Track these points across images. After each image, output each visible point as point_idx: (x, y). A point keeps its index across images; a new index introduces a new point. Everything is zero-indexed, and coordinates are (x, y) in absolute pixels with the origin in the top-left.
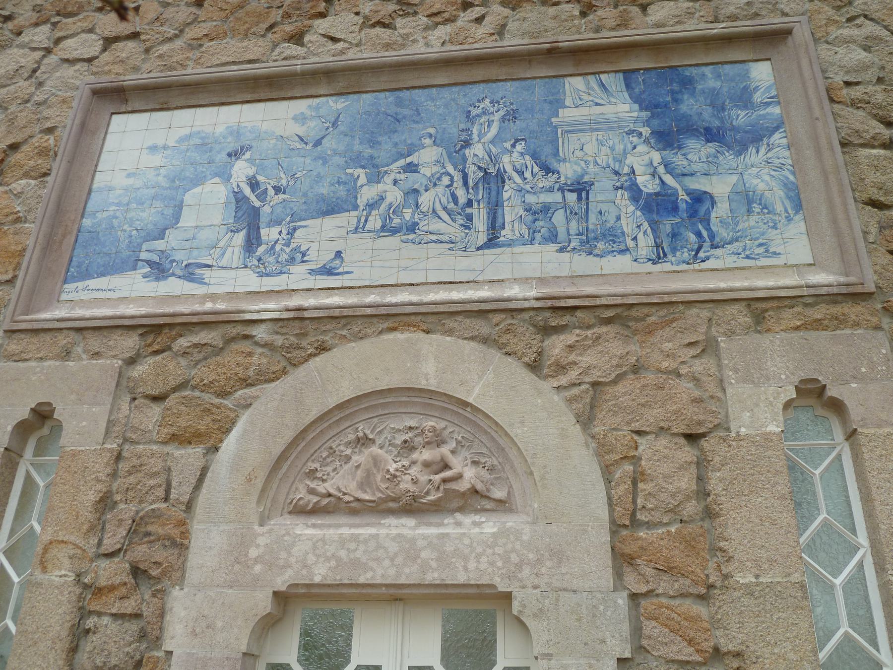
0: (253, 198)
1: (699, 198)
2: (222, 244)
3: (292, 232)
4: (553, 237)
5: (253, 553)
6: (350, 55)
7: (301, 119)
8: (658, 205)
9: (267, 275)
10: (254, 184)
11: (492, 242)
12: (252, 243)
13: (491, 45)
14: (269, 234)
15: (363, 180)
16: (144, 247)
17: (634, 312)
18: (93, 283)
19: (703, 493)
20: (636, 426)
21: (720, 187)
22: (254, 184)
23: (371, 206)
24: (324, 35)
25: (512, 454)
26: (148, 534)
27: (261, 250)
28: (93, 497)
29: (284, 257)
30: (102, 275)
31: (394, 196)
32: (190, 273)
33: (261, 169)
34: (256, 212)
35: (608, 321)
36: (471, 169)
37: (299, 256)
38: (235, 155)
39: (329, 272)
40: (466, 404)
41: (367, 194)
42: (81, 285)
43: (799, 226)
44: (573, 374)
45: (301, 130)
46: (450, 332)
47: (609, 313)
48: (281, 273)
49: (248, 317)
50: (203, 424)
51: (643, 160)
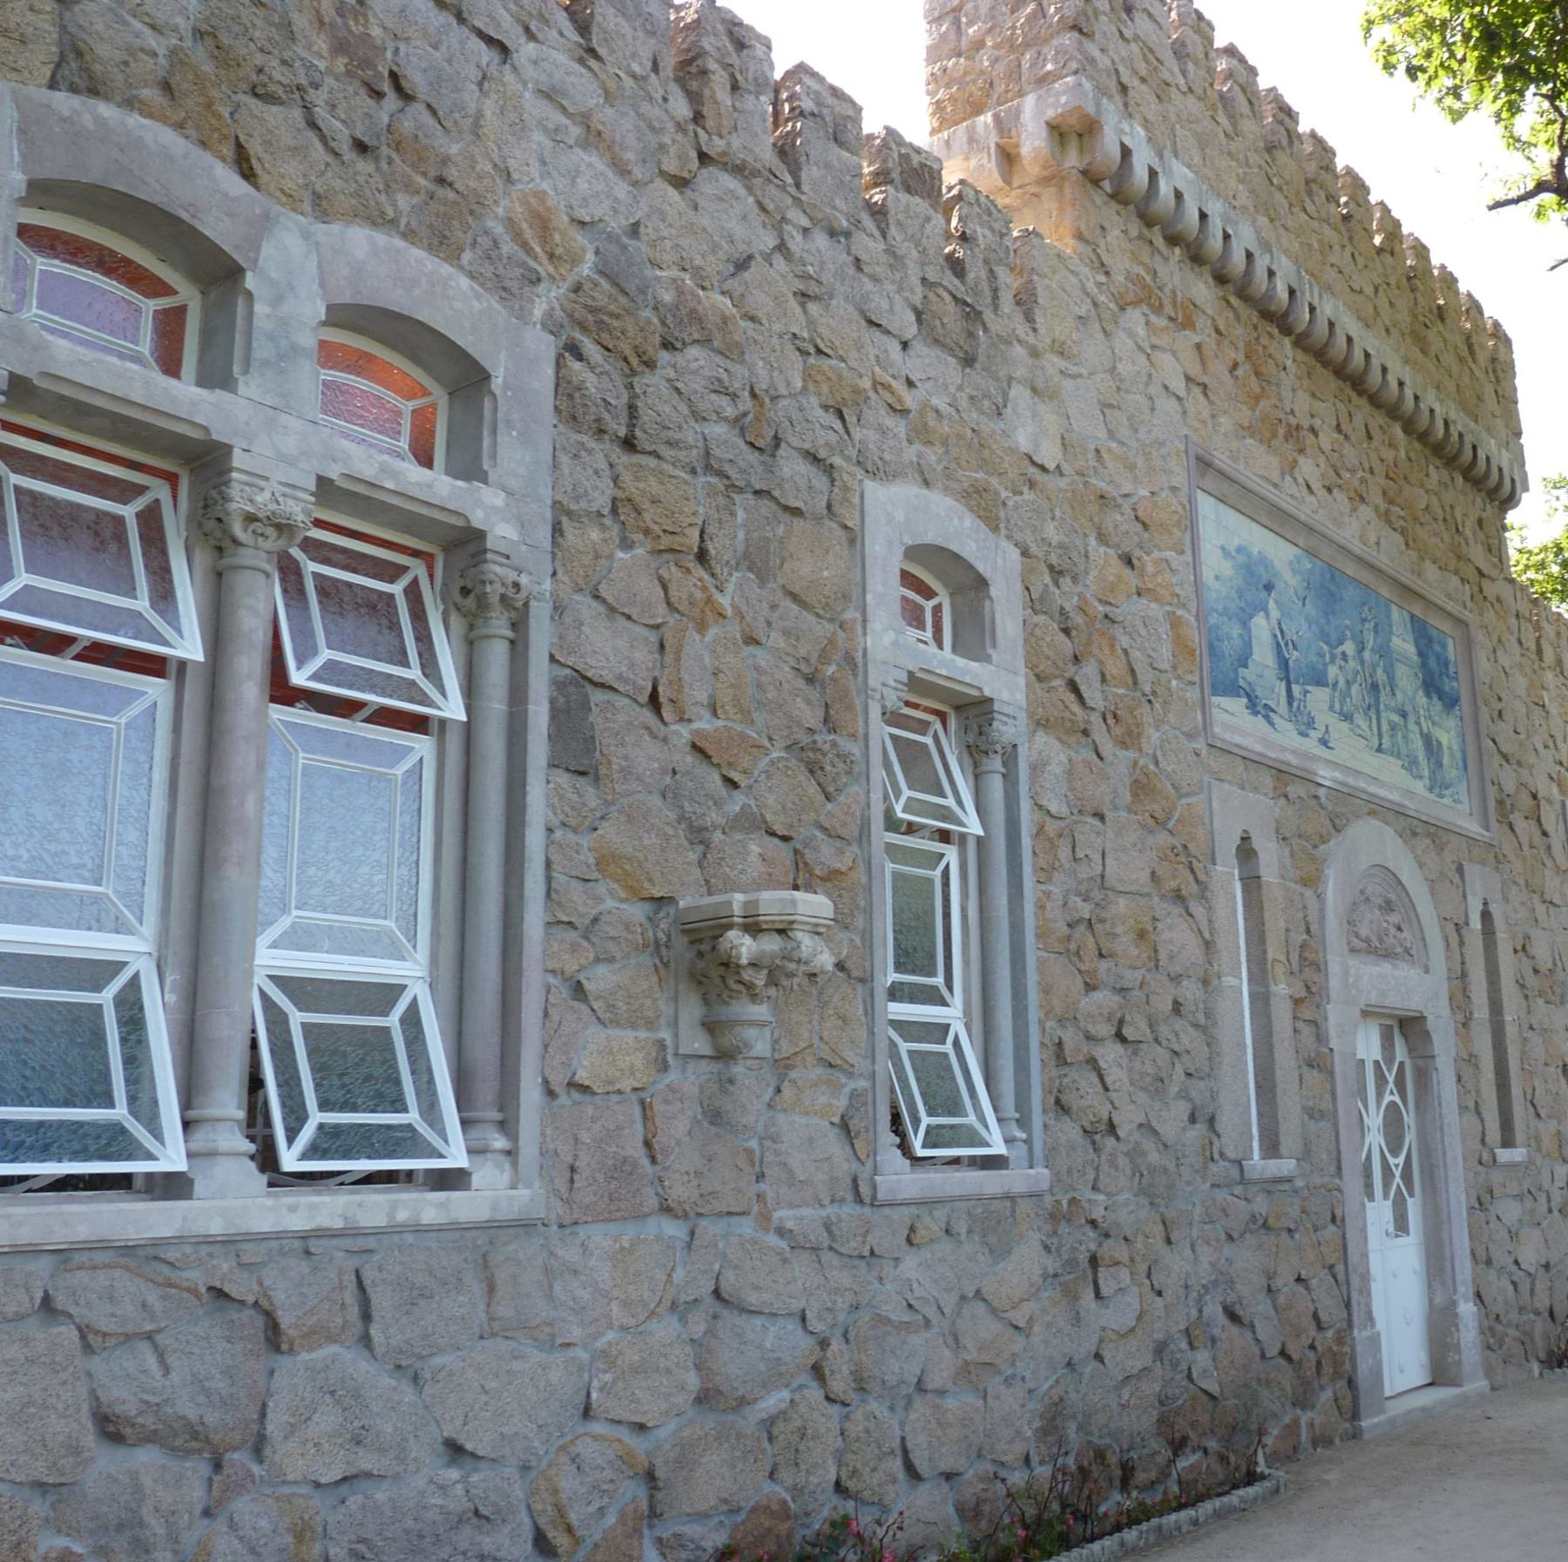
3: (1306, 692)
4: (1398, 756)
10: (1282, 632)
11: (1379, 750)
14: (1296, 689)
15: (1328, 659)
21: (1445, 742)
22: (1282, 632)
28: (1282, 925)
31: (1342, 684)
34: (1287, 661)
35: (1429, 834)
40: (1401, 883)
41: (1333, 672)
47: (1432, 830)
51: (1422, 700)
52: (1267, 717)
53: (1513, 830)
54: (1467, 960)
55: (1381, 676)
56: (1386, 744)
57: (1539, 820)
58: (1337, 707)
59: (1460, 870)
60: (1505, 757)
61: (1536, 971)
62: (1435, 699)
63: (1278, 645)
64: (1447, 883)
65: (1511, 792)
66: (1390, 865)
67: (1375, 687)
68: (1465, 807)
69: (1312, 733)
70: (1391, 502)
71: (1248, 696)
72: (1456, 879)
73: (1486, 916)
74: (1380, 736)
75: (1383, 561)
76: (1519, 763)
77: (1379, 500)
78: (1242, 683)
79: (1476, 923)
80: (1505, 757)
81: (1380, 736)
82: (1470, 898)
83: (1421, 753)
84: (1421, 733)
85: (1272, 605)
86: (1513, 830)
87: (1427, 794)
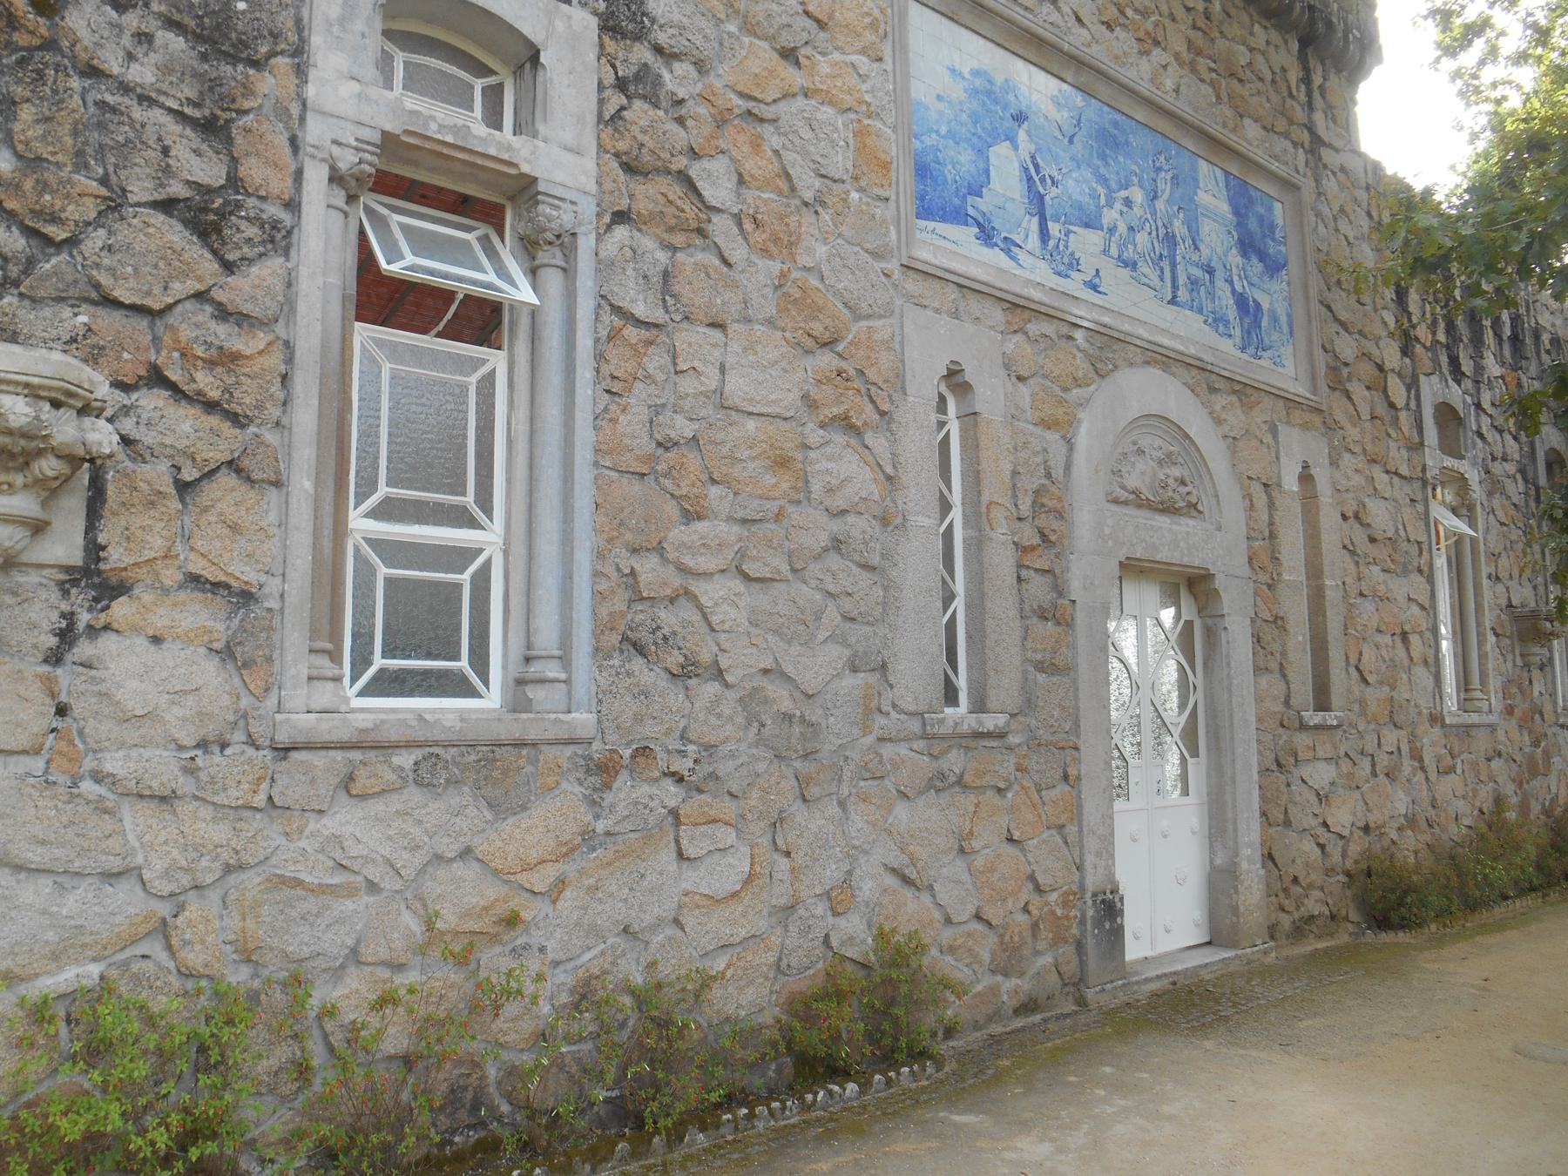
0: (1036, 178)
1: (1258, 306)
2: (1024, 225)
3: (1068, 233)
4: (1200, 311)
5: (1107, 531)
6: (1094, 50)
7: (1056, 102)
8: (1242, 302)
9: (1059, 274)
10: (1036, 166)
11: (1173, 301)
12: (1044, 234)
13: (1168, 100)
14: (1054, 228)
15: (1103, 202)
16: (969, 199)
17: (1249, 391)
18: (942, 228)
19: (1271, 524)
20: (1250, 473)
21: (1265, 306)
22: (1036, 166)
23: (1112, 230)
24: (1075, 13)
25: (1206, 479)
26: (1043, 505)
27: (1051, 243)
28: (1007, 467)
29: (1066, 260)
30: (944, 220)
31: (1122, 228)
32: (1009, 246)
33: (1038, 149)
34: (1041, 197)
35: (1235, 392)
36: (1160, 224)
37: (1074, 264)
38: (1020, 118)
39: (1095, 288)
40: (1188, 437)
41: (1109, 216)
42: (931, 225)
43: (1290, 349)
44: (1226, 428)
45: (1058, 116)
46: (1173, 374)
47: (1237, 387)
48: (1067, 276)
49: (1074, 320)
50: (1059, 413)
51: (1235, 259)
52: (1008, 252)
53: (1349, 398)
54: (1277, 520)
55: (1179, 227)
56: (1183, 295)
57: (1385, 391)
58: (1114, 251)
59: (1274, 431)
60: (1343, 325)
61: (1372, 540)
62: (1255, 260)
63: (1030, 179)
64: (1255, 443)
65: (1350, 360)
66: (1173, 416)
67: (1170, 240)
68: (1290, 370)
69: (1074, 274)
70: (1199, 53)
71: (979, 224)
72: (1268, 439)
73: (1306, 478)
74: (1175, 287)
75: (1183, 108)
76: (1360, 332)
77: (1181, 47)
78: (971, 211)
79: (1291, 483)
80: (1343, 325)
81: (1175, 287)
82: (1284, 460)
83: (1232, 314)
84: (1233, 291)
85: (1022, 136)
86: (1349, 398)
87: (1238, 353)
